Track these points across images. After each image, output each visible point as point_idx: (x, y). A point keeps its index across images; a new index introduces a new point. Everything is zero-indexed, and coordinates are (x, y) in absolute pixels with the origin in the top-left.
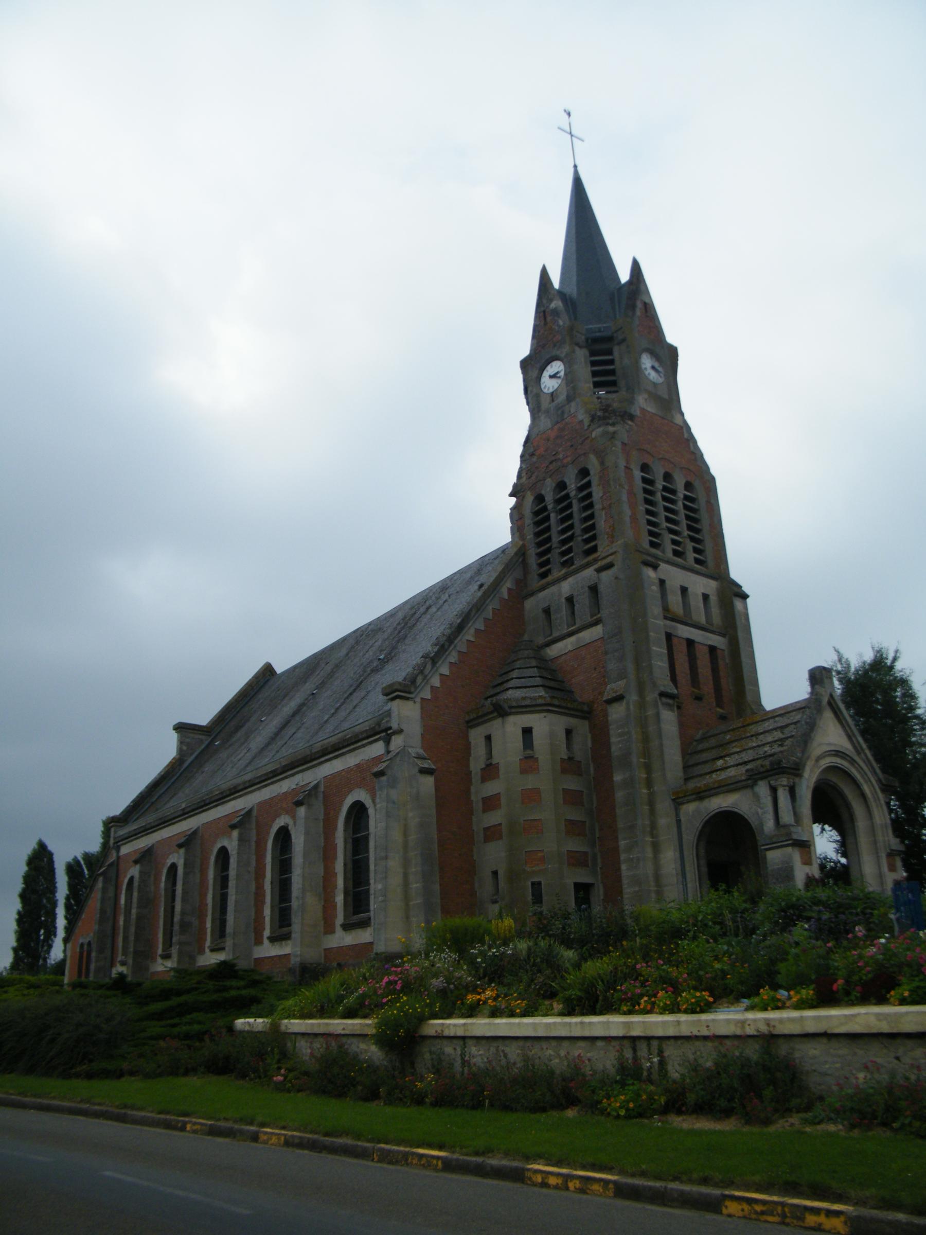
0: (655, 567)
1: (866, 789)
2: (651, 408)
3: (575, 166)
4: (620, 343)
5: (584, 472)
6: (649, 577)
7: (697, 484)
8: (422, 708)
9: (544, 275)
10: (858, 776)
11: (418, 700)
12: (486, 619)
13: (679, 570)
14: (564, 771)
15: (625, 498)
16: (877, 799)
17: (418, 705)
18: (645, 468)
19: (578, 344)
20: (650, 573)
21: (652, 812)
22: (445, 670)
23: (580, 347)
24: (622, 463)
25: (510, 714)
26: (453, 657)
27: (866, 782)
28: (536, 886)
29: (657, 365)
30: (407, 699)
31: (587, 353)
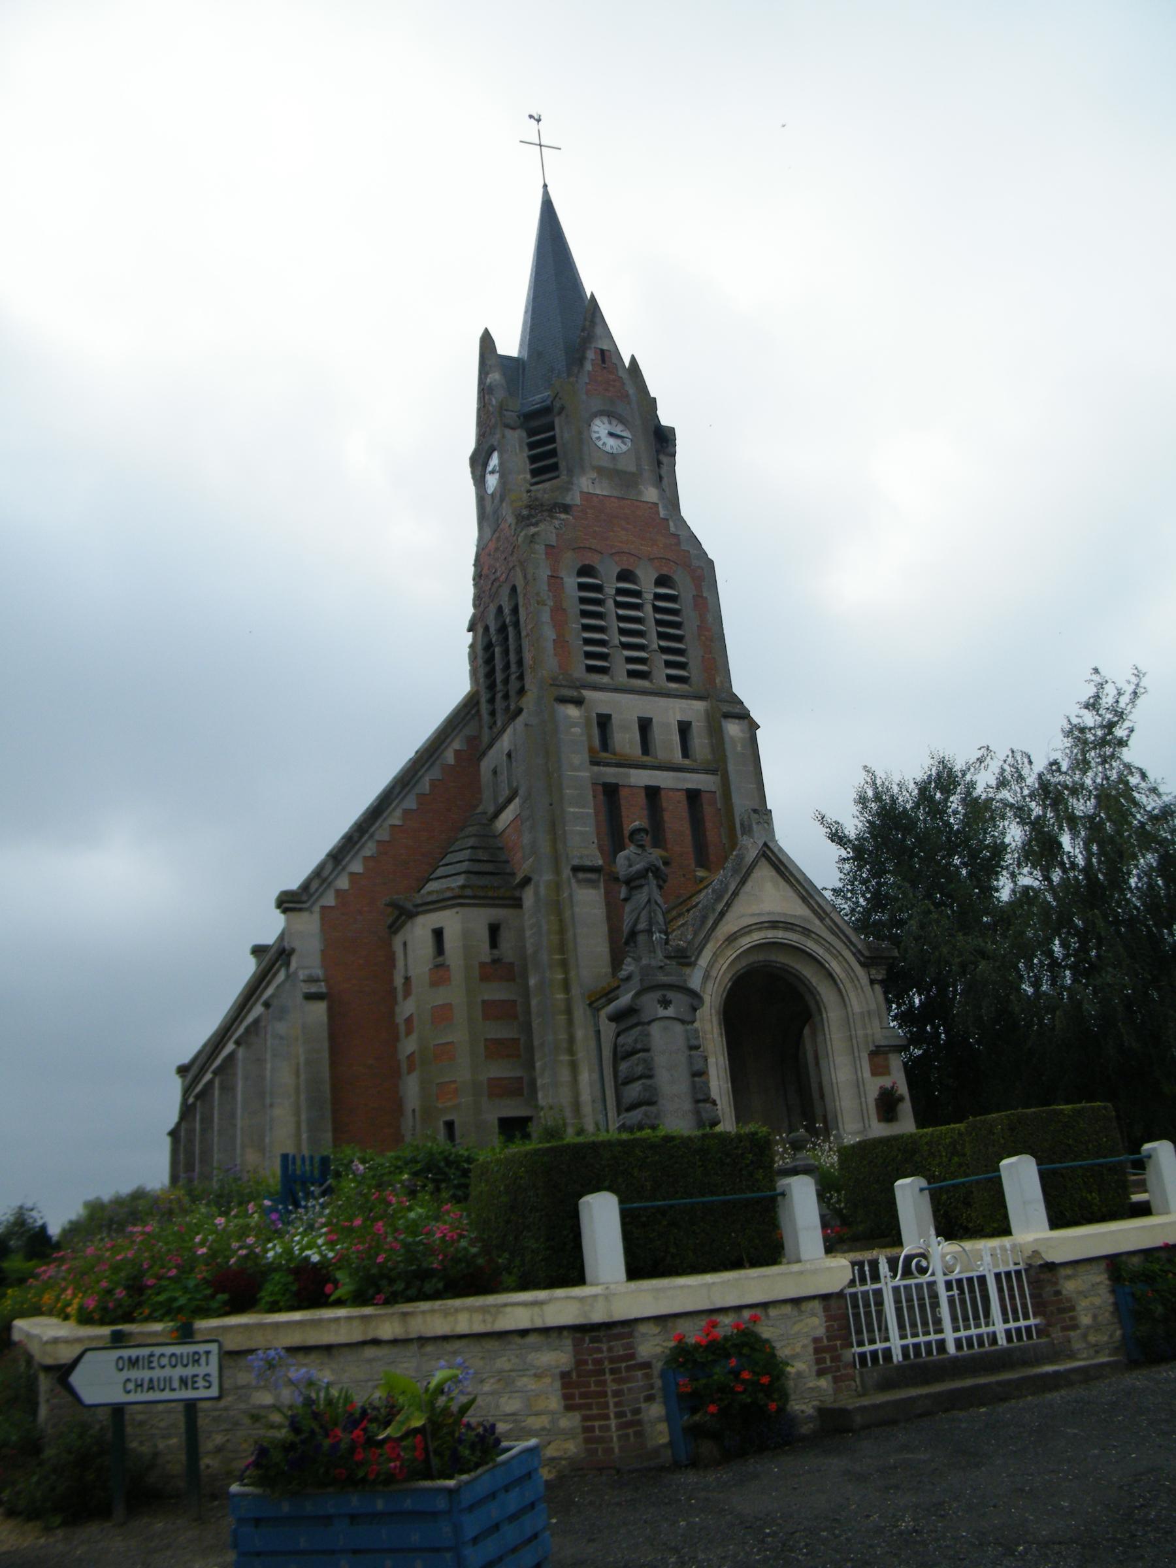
0: (579, 702)
1: (835, 967)
2: (601, 489)
3: (545, 186)
4: (559, 413)
5: (514, 589)
6: (567, 717)
7: (679, 576)
8: (322, 919)
9: (487, 341)
10: (819, 951)
11: (317, 909)
12: (421, 796)
13: (637, 697)
14: (484, 978)
15: (546, 617)
16: (854, 978)
17: (316, 917)
18: (586, 570)
19: (507, 426)
20: (572, 711)
21: (570, 1022)
22: (357, 867)
23: (513, 429)
24: (544, 573)
25: (418, 914)
26: (370, 849)
27: (835, 957)
28: (450, 1125)
29: (618, 430)
30: (300, 910)
31: (524, 434)
